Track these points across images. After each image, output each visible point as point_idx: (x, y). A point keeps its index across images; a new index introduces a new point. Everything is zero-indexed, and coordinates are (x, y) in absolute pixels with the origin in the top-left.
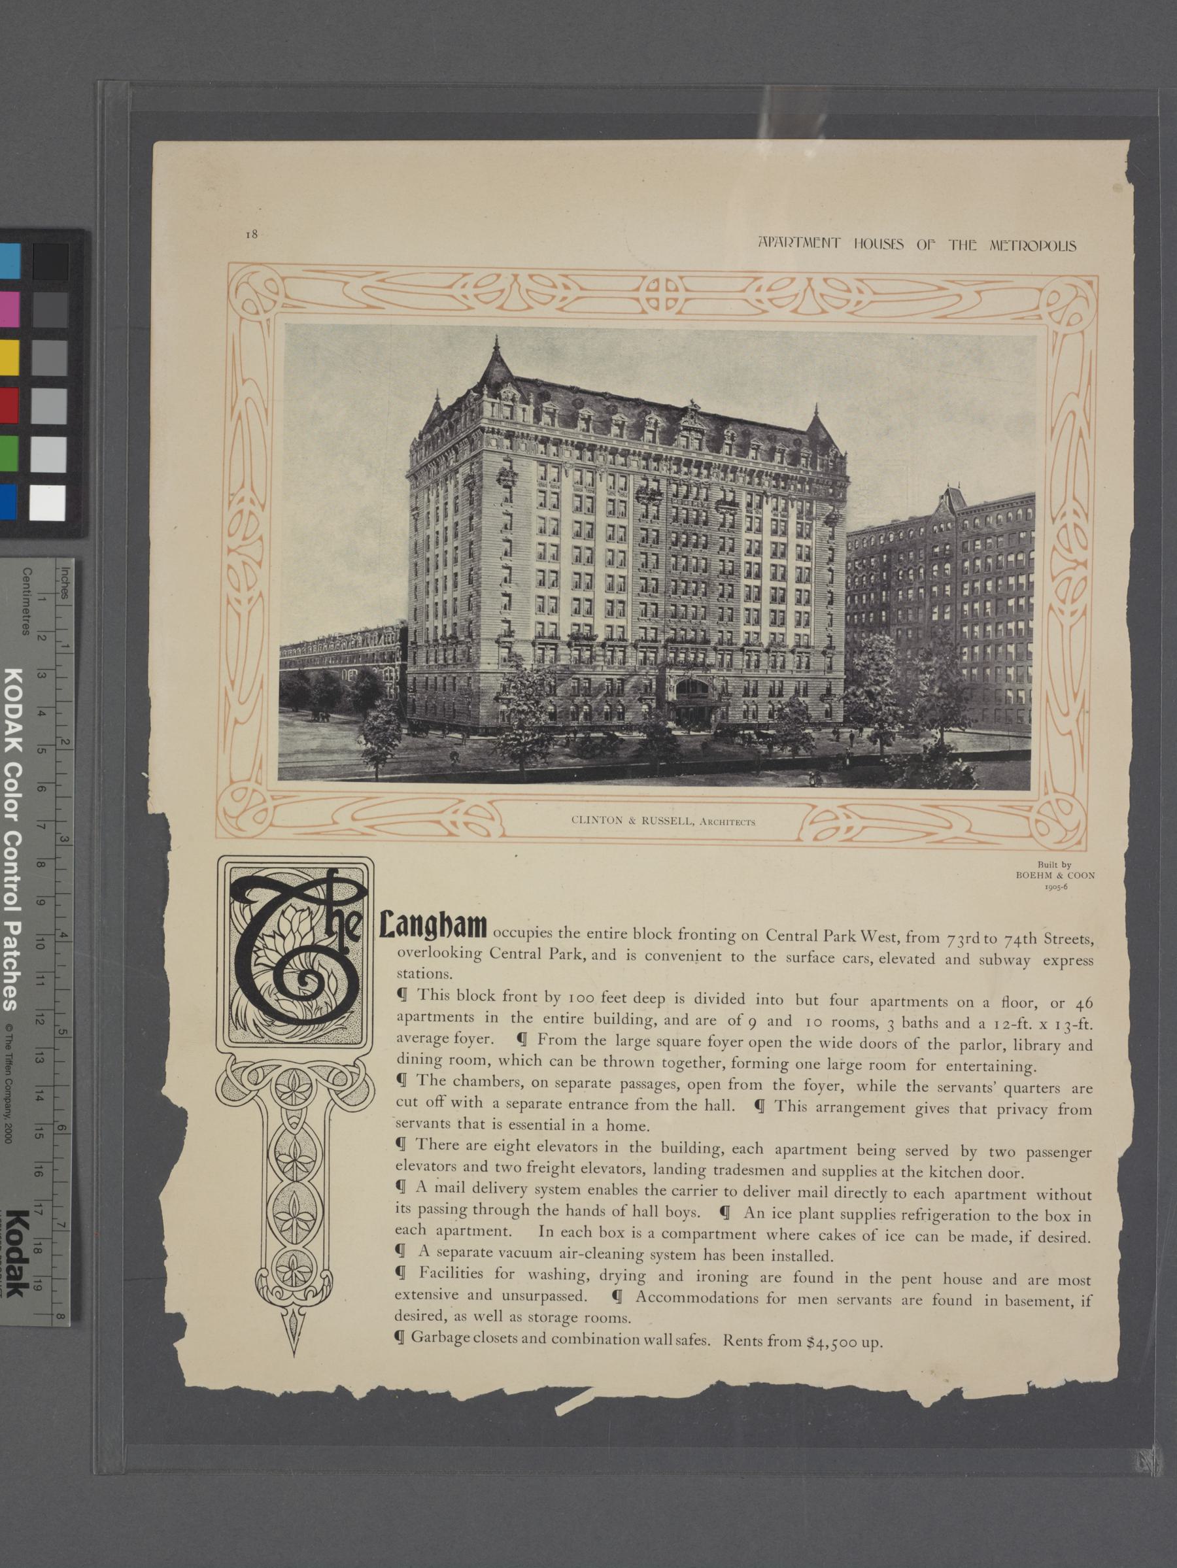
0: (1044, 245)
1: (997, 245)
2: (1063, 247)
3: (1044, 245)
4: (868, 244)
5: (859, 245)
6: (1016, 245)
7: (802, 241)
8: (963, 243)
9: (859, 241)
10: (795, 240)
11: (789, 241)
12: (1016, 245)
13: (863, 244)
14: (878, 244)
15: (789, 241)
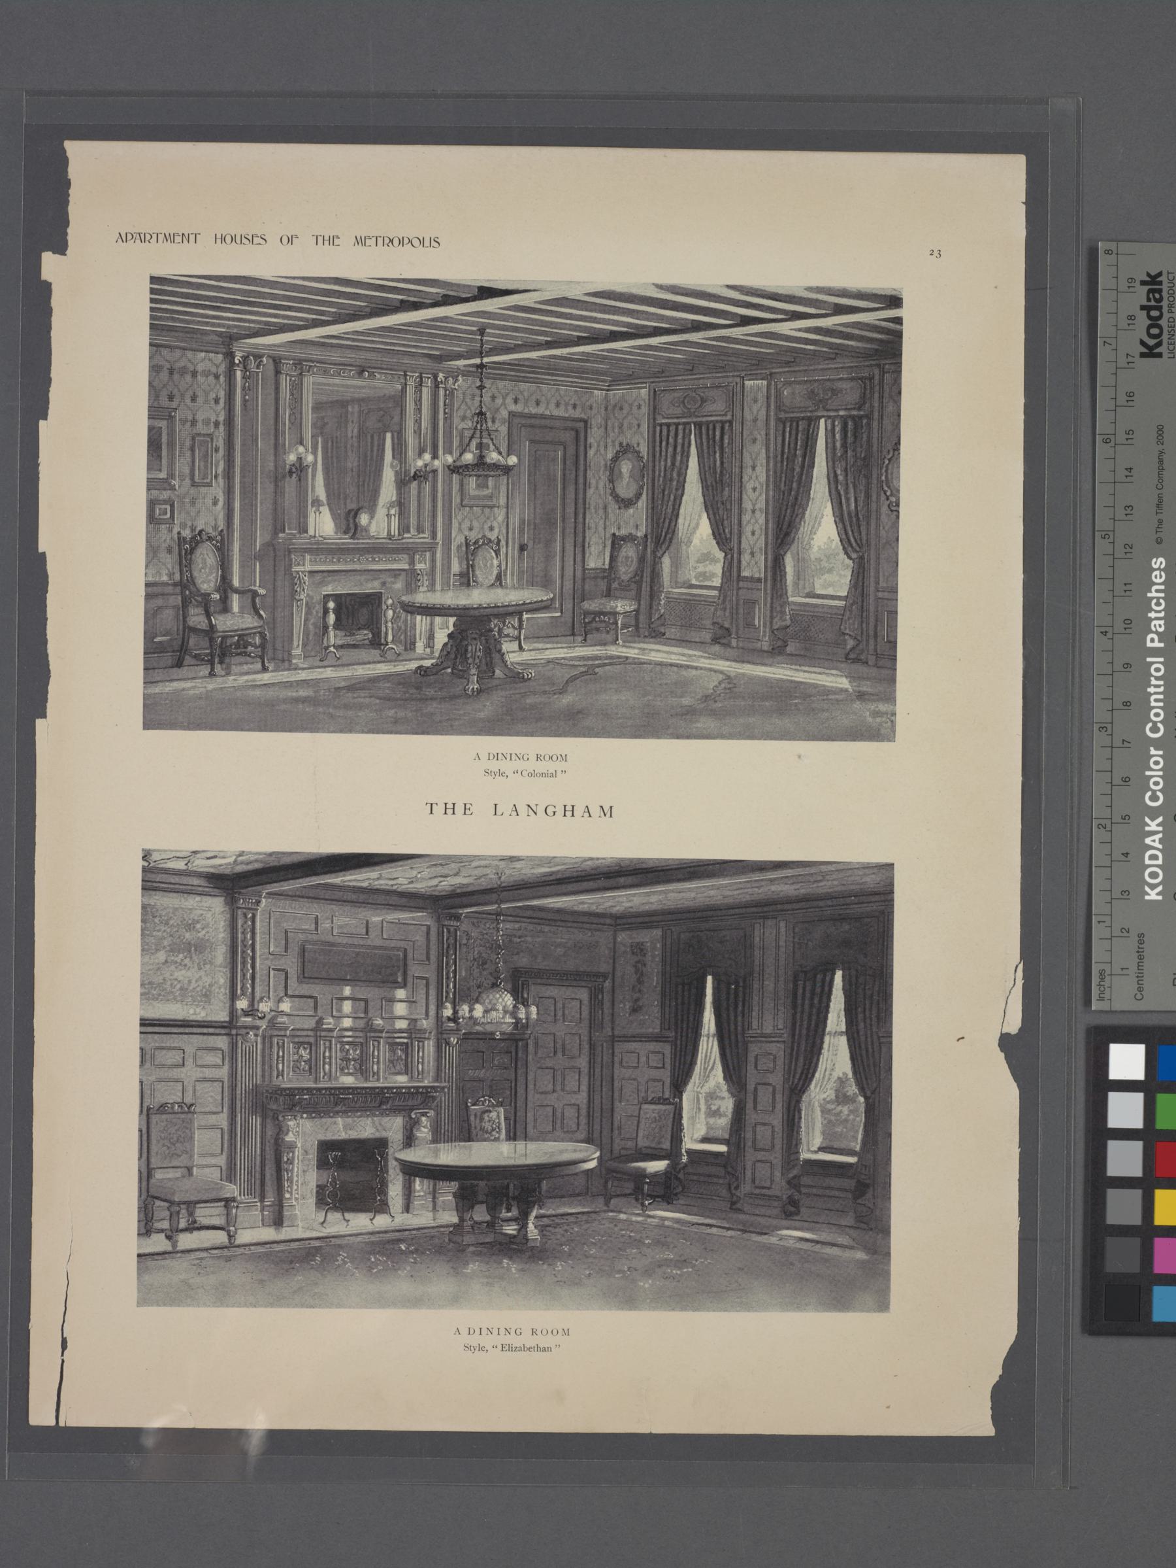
0: (406, 241)
1: (360, 241)
3: (406, 241)
4: (228, 239)
5: (219, 241)
6: (380, 241)
7: (161, 237)
8: (327, 238)
9: (219, 236)
10: (154, 236)
11: (148, 237)
12: (380, 241)
13: (223, 239)
14: (238, 240)
15: (148, 237)
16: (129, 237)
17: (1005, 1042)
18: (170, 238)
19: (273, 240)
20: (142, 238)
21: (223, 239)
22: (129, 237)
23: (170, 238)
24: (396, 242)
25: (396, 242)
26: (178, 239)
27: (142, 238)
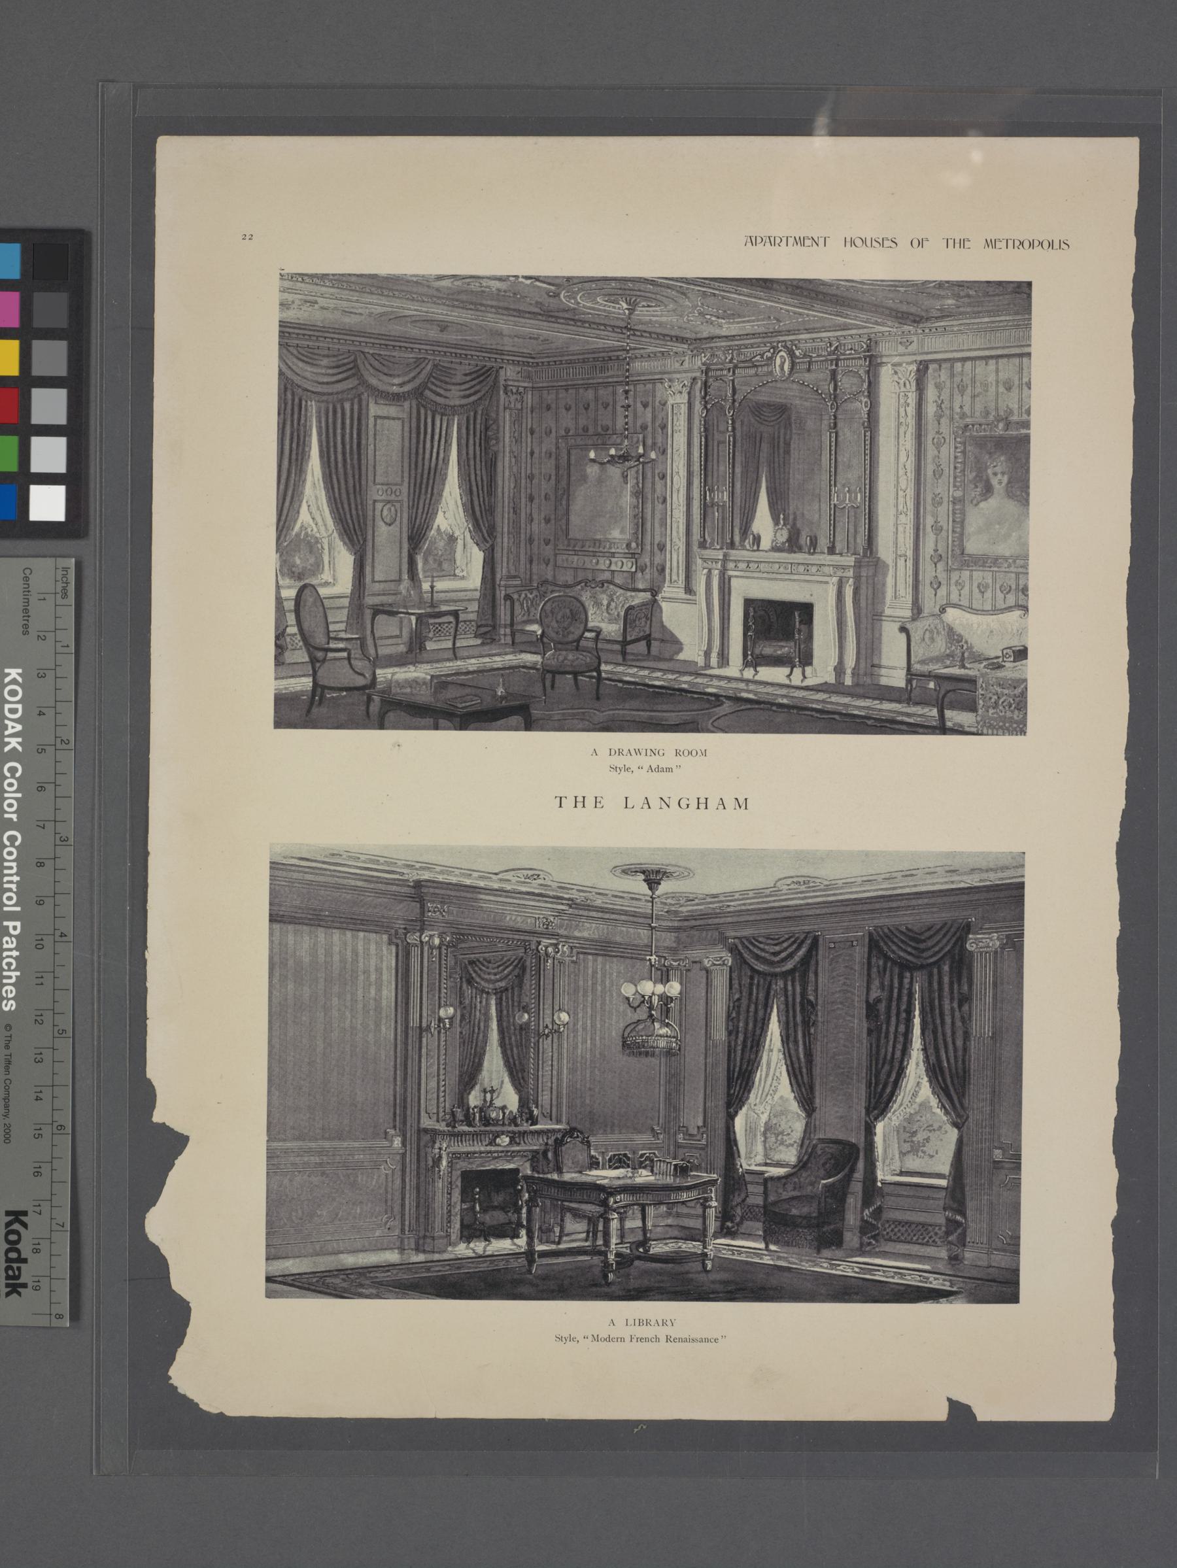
0: (1036, 243)
1: (991, 244)
2: (1056, 245)
3: (1036, 243)
5: (848, 244)
6: (1010, 243)
7: (791, 241)
8: (957, 241)
9: (848, 240)
10: (784, 240)
12: (1010, 243)
14: (869, 243)
15: (778, 240)
16: (759, 240)
18: (800, 241)
19: (904, 243)
21: (853, 243)
22: (759, 240)
23: (800, 241)
24: (1026, 244)
25: (1026, 244)
26: (808, 242)
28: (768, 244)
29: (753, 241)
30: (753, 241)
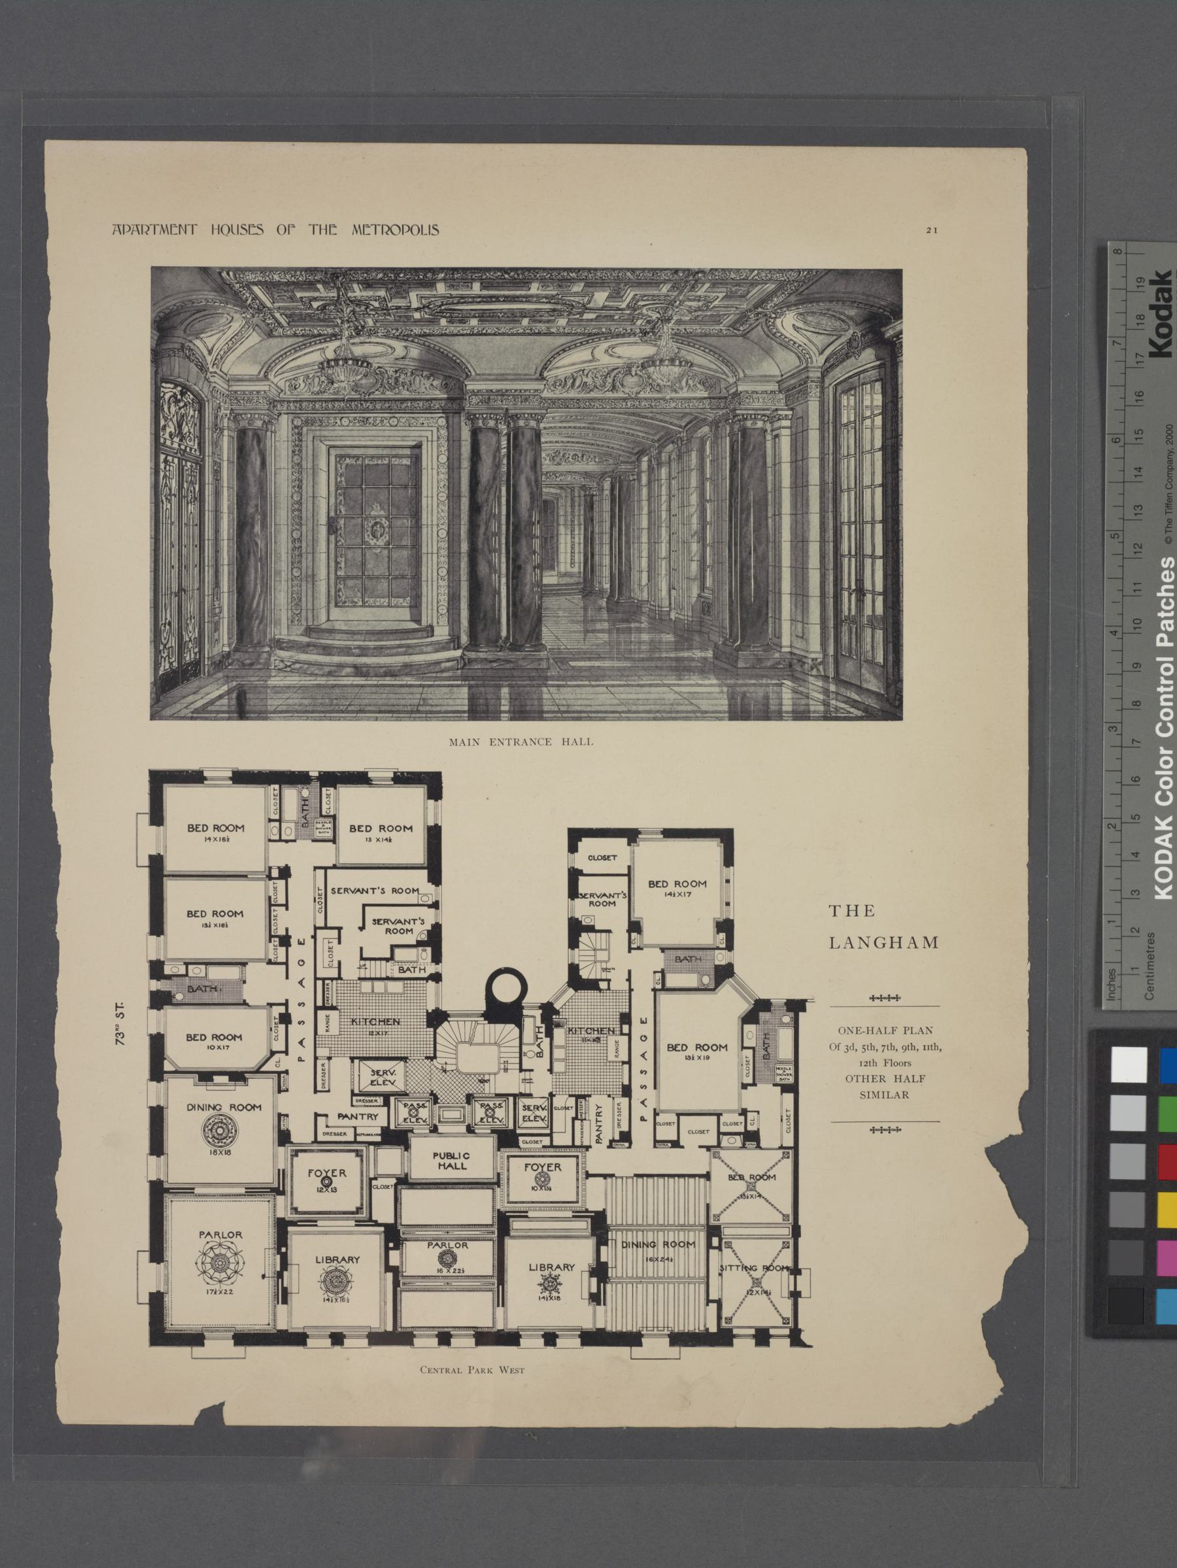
0: (406, 229)
1: (359, 230)
2: (426, 230)
3: (406, 229)
4: (225, 230)
5: (216, 231)
6: (379, 229)
7: (158, 229)
8: (323, 227)
9: (216, 227)
10: (152, 228)
11: (145, 229)
12: (379, 229)
13: (220, 230)
14: (235, 231)
15: (145, 229)
16: (127, 228)
17: (1000, 1155)
19: (270, 228)
20: (139, 229)
21: (220, 230)
22: (127, 228)
26: (175, 230)
27: (139, 229)
28: (136, 233)
29: (120, 229)
30: (120, 229)
